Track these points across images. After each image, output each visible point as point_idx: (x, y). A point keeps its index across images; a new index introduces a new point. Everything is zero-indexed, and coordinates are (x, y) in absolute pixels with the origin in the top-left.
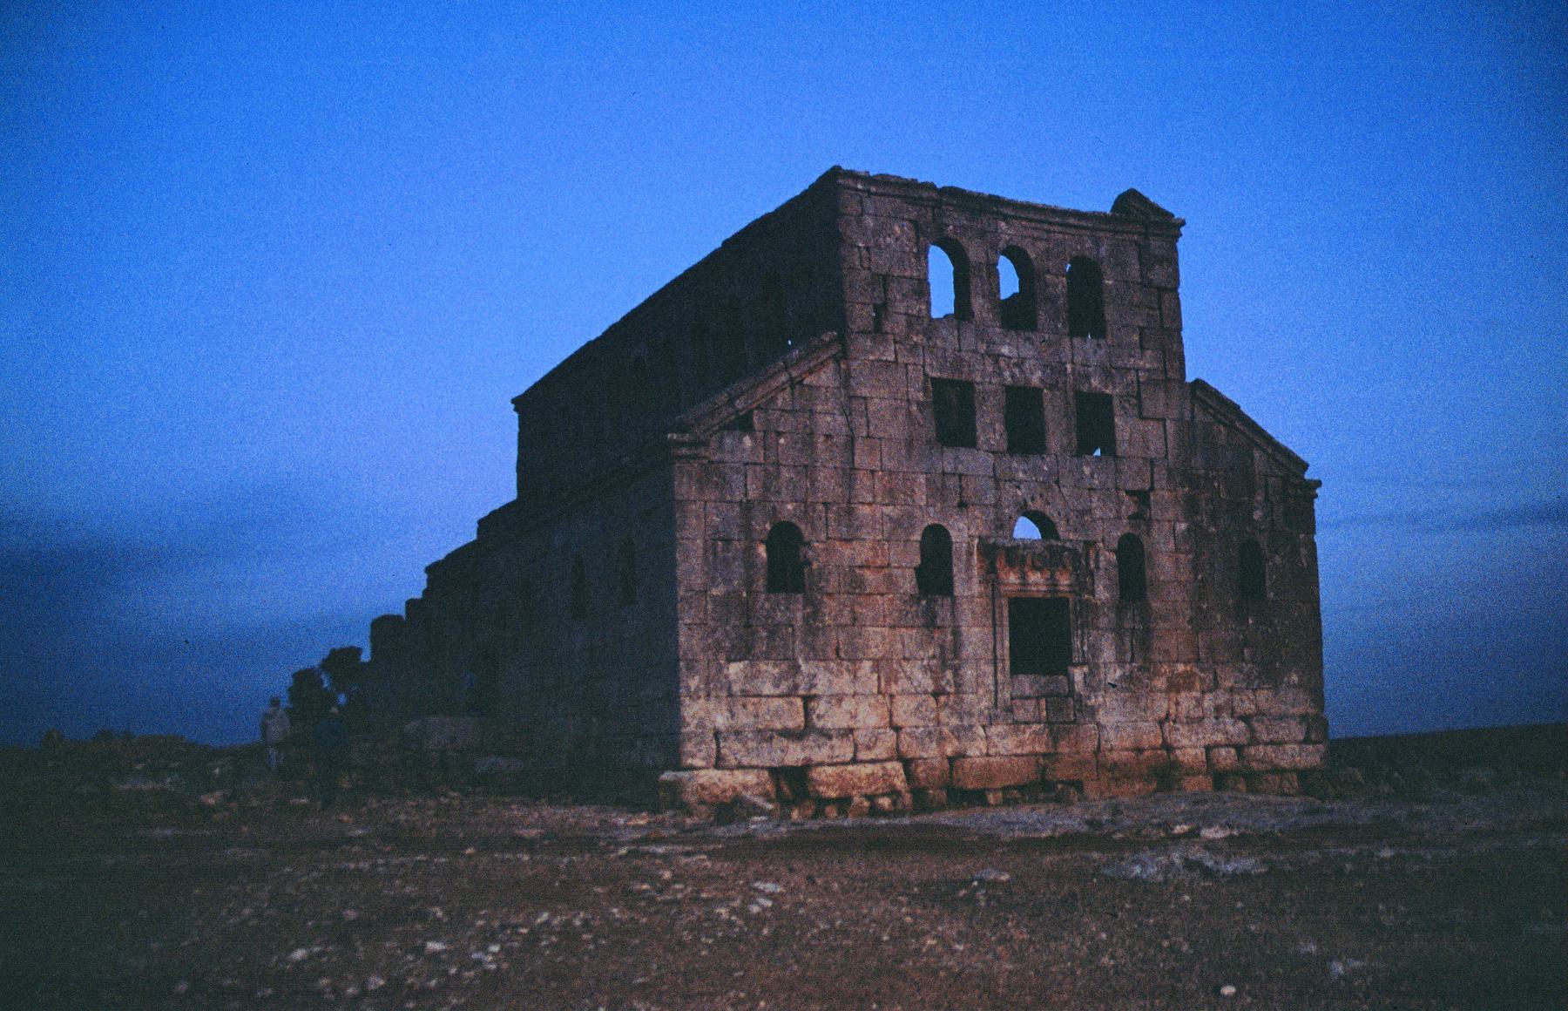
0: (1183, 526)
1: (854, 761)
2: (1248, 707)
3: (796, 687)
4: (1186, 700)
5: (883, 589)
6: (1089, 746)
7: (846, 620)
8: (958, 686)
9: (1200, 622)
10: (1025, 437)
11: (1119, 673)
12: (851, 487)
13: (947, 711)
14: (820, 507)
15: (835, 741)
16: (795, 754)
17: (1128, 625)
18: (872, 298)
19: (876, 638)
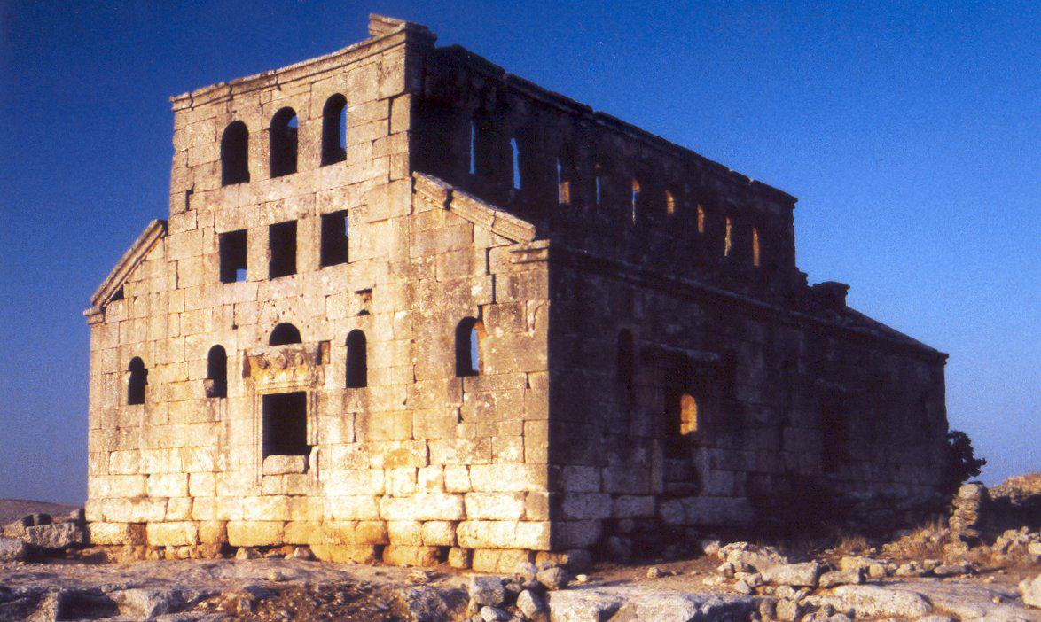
0: (401, 315)
1: (164, 522)
5: (185, 397)
6: (314, 516)
7: (165, 421)
8: (228, 465)
9: (414, 401)
14: (153, 344)
16: (137, 514)
17: (351, 410)
19: (180, 433)
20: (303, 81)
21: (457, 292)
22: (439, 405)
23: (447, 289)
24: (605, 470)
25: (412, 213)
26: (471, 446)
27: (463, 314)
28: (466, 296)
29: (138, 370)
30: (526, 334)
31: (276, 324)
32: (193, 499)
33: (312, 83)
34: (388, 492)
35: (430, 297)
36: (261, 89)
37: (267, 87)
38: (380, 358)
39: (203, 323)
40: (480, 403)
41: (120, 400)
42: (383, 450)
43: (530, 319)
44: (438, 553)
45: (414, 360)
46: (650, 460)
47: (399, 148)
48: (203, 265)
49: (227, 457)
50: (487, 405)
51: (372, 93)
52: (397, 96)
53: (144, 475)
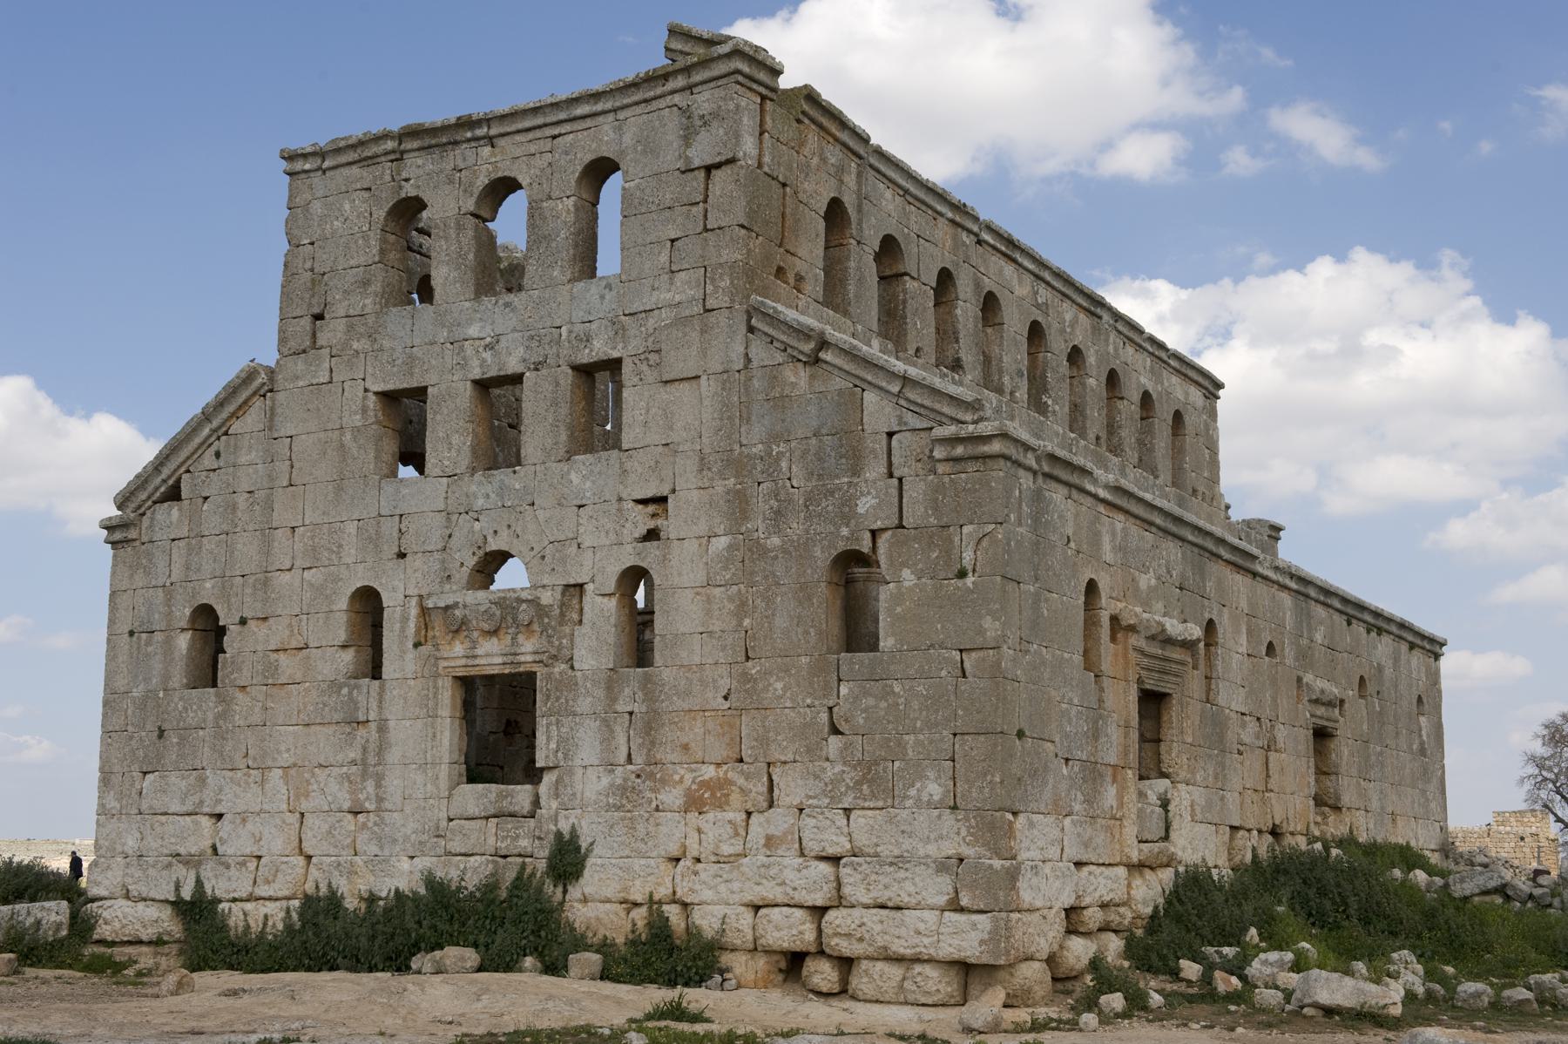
0: (721, 543)
2: (837, 843)
3: (202, 802)
4: (716, 828)
8: (380, 800)
9: (744, 698)
10: (499, 445)
11: (605, 781)
12: (268, 553)
13: (365, 835)
15: (233, 872)
17: (622, 706)
18: (310, 305)
20: (538, 134)
21: (829, 505)
22: (789, 697)
23: (809, 499)
24: (1067, 821)
25: (746, 367)
26: (851, 776)
27: (841, 546)
28: (846, 512)
29: (209, 628)
30: (960, 583)
31: (481, 553)
32: (309, 858)
33: (554, 137)
34: (693, 850)
35: (778, 513)
36: (456, 143)
37: (469, 140)
38: (684, 615)
39: (340, 546)
40: (871, 701)
41: (166, 677)
42: (681, 780)
43: (968, 557)
44: (783, 965)
45: (747, 622)
46: (1121, 805)
47: (725, 252)
48: (342, 446)
49: (378, 786)
50: (883, 704)
51: (670, 159)
52: (718, 166)
53: (211, 815)
